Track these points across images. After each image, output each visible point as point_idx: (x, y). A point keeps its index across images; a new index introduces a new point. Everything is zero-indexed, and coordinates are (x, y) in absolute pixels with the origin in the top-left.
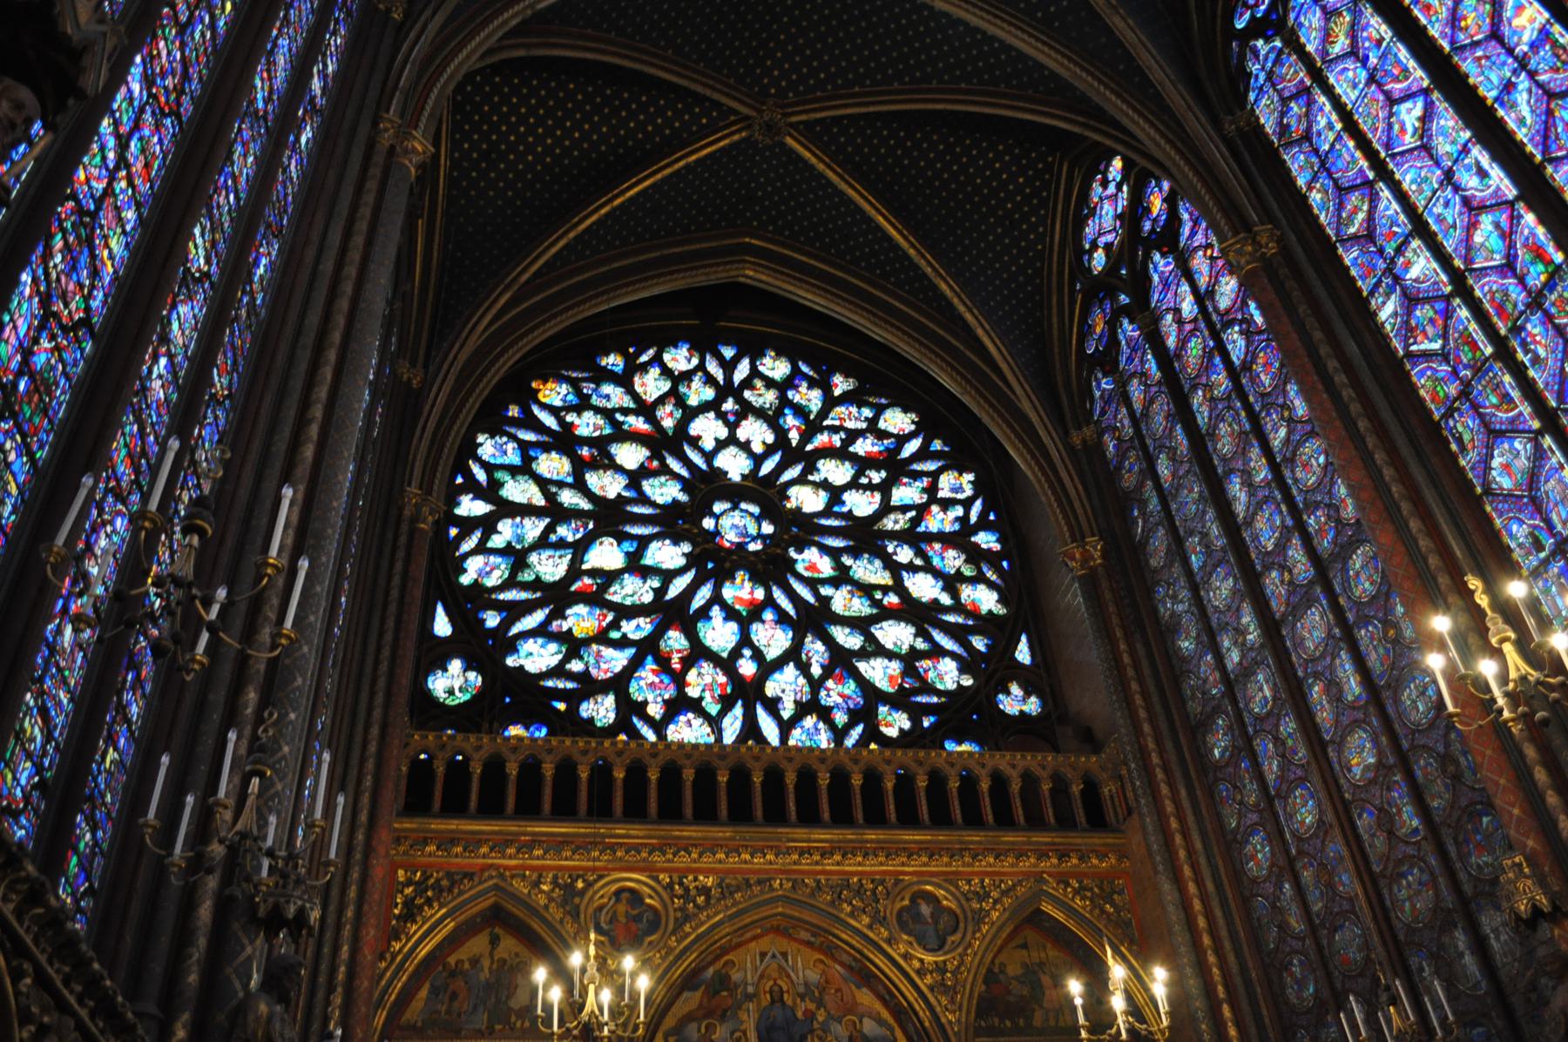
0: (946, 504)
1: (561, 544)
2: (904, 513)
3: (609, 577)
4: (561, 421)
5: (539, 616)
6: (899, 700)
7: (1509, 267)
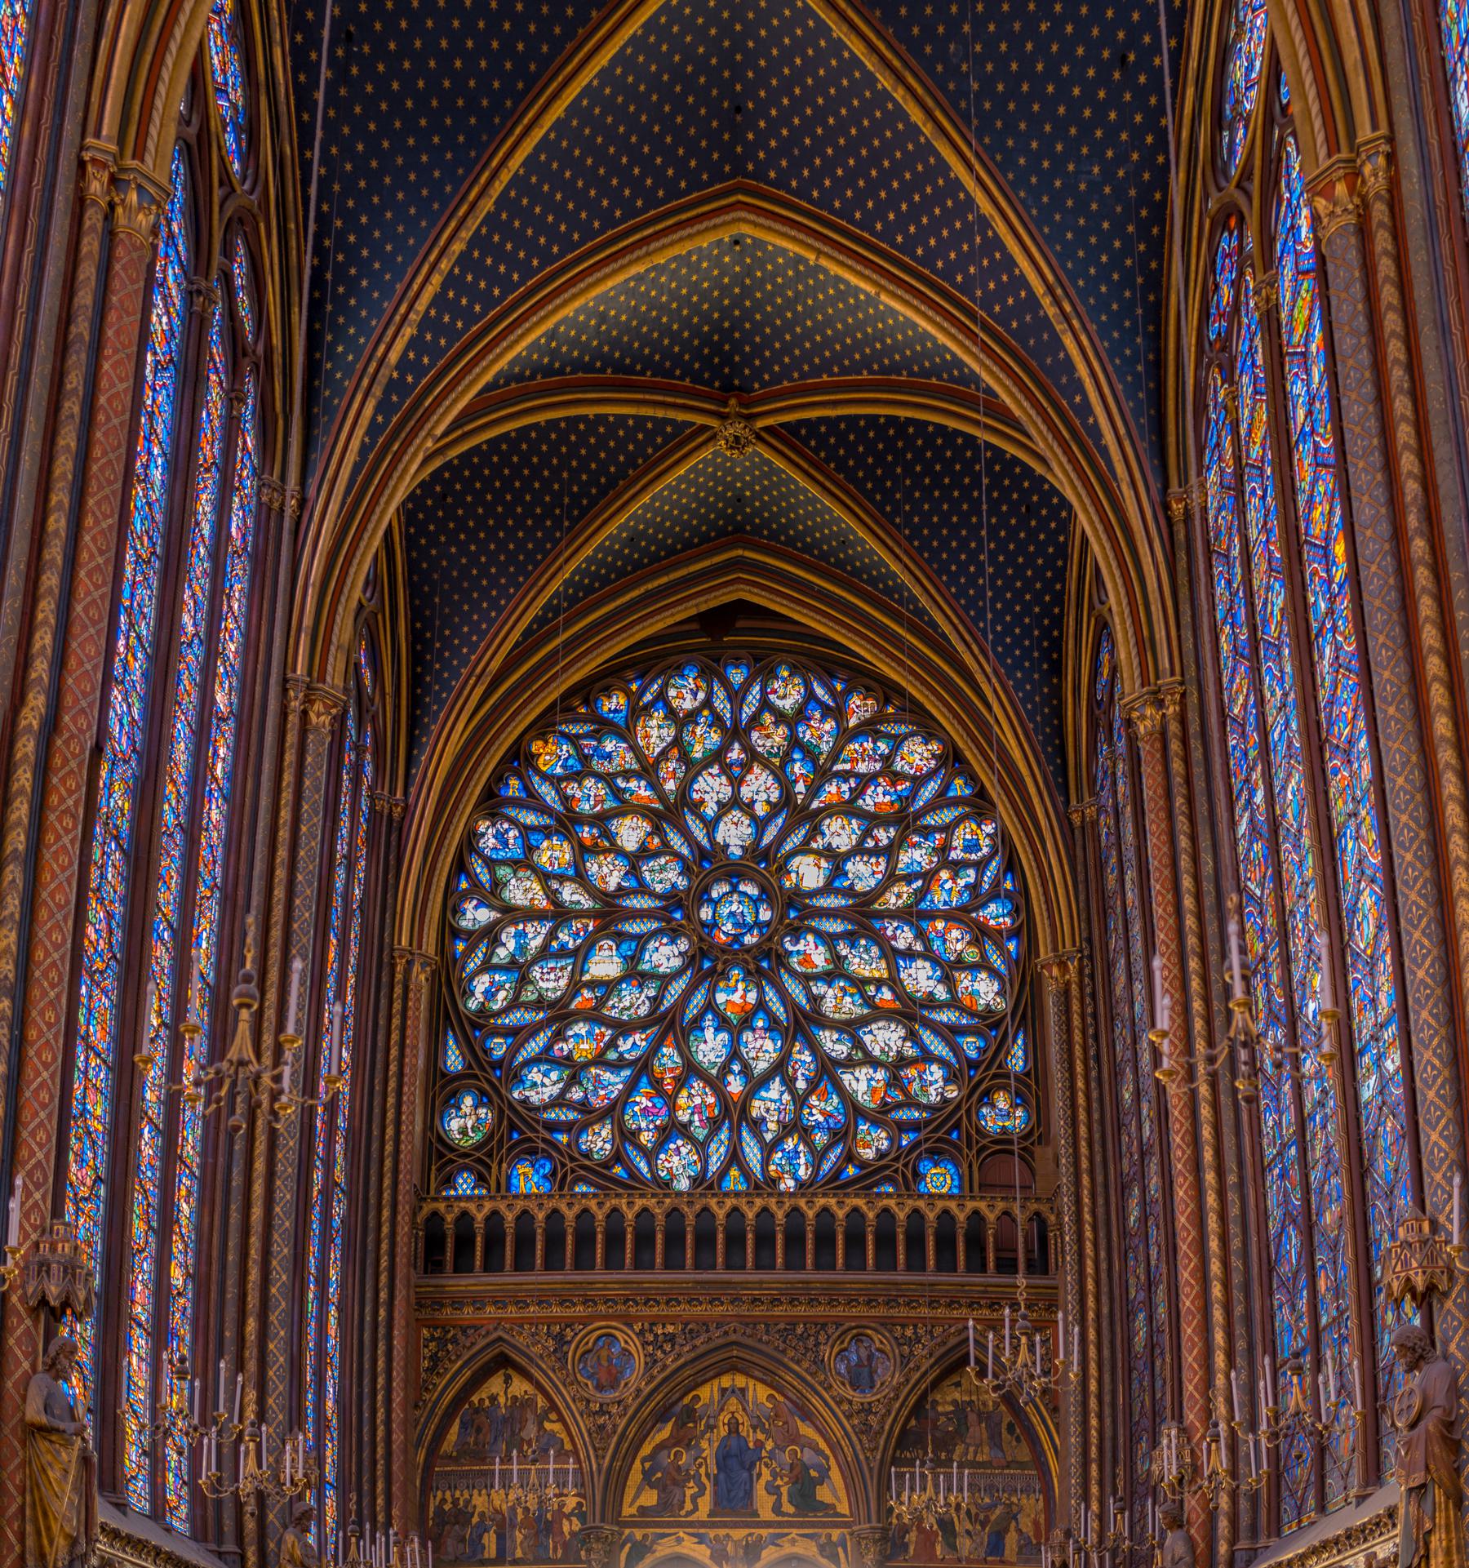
0: (957, 867)
1: (563, 953)
2: (909, 883)
3: (609, 987)
5: (542, 1039)
6: (879, 1117)
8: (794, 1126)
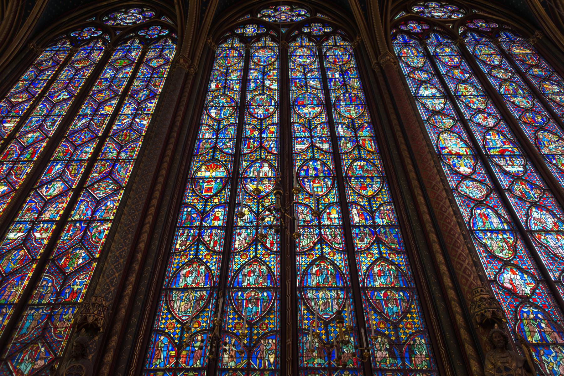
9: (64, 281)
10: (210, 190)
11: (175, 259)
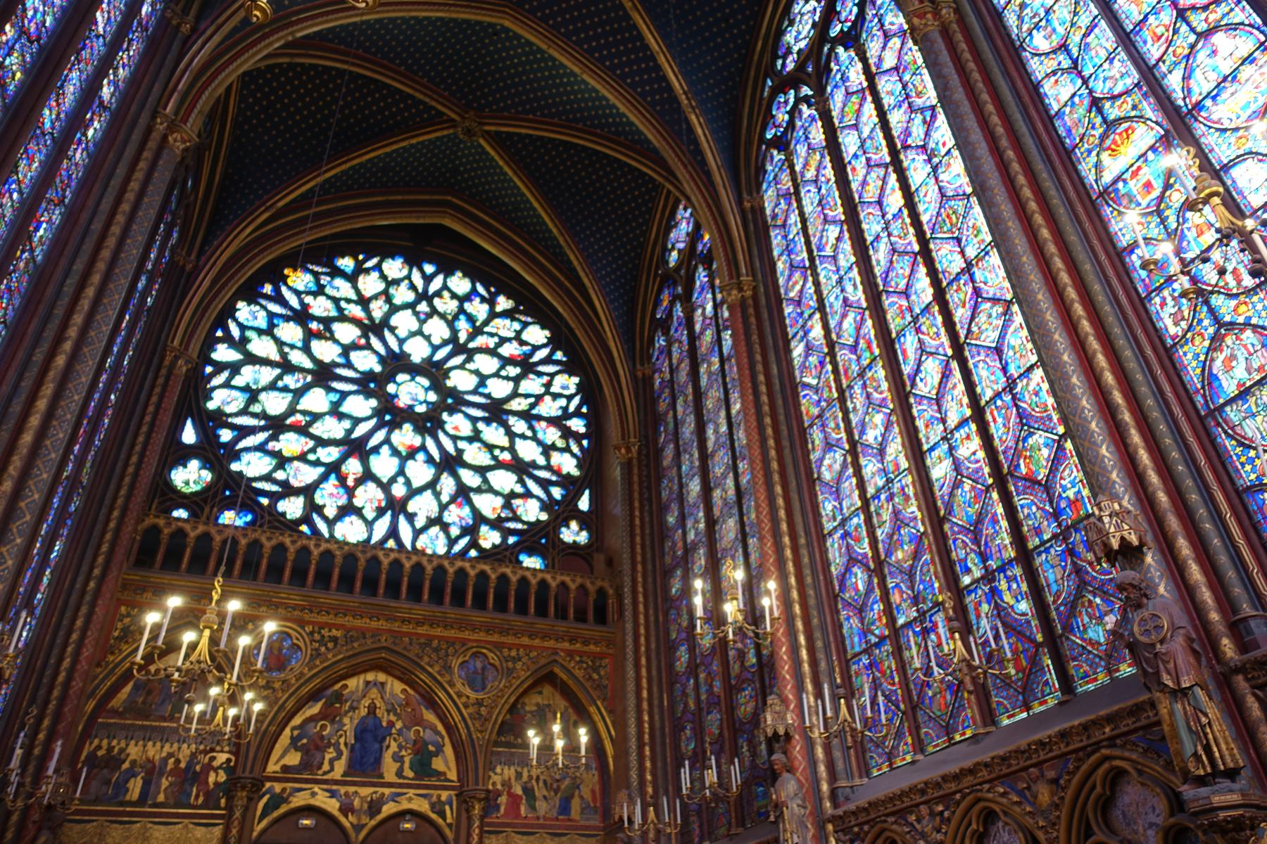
0: (556, 396)
1: (285, 389)
3: (316, 417)
4: (301, 302)
5: (261, 437)
6: (496, 524)
7: (854, 348)
8: (437, 521)
9: (1048, 494)
10: (1148, 186)
11: (1185, 354)
